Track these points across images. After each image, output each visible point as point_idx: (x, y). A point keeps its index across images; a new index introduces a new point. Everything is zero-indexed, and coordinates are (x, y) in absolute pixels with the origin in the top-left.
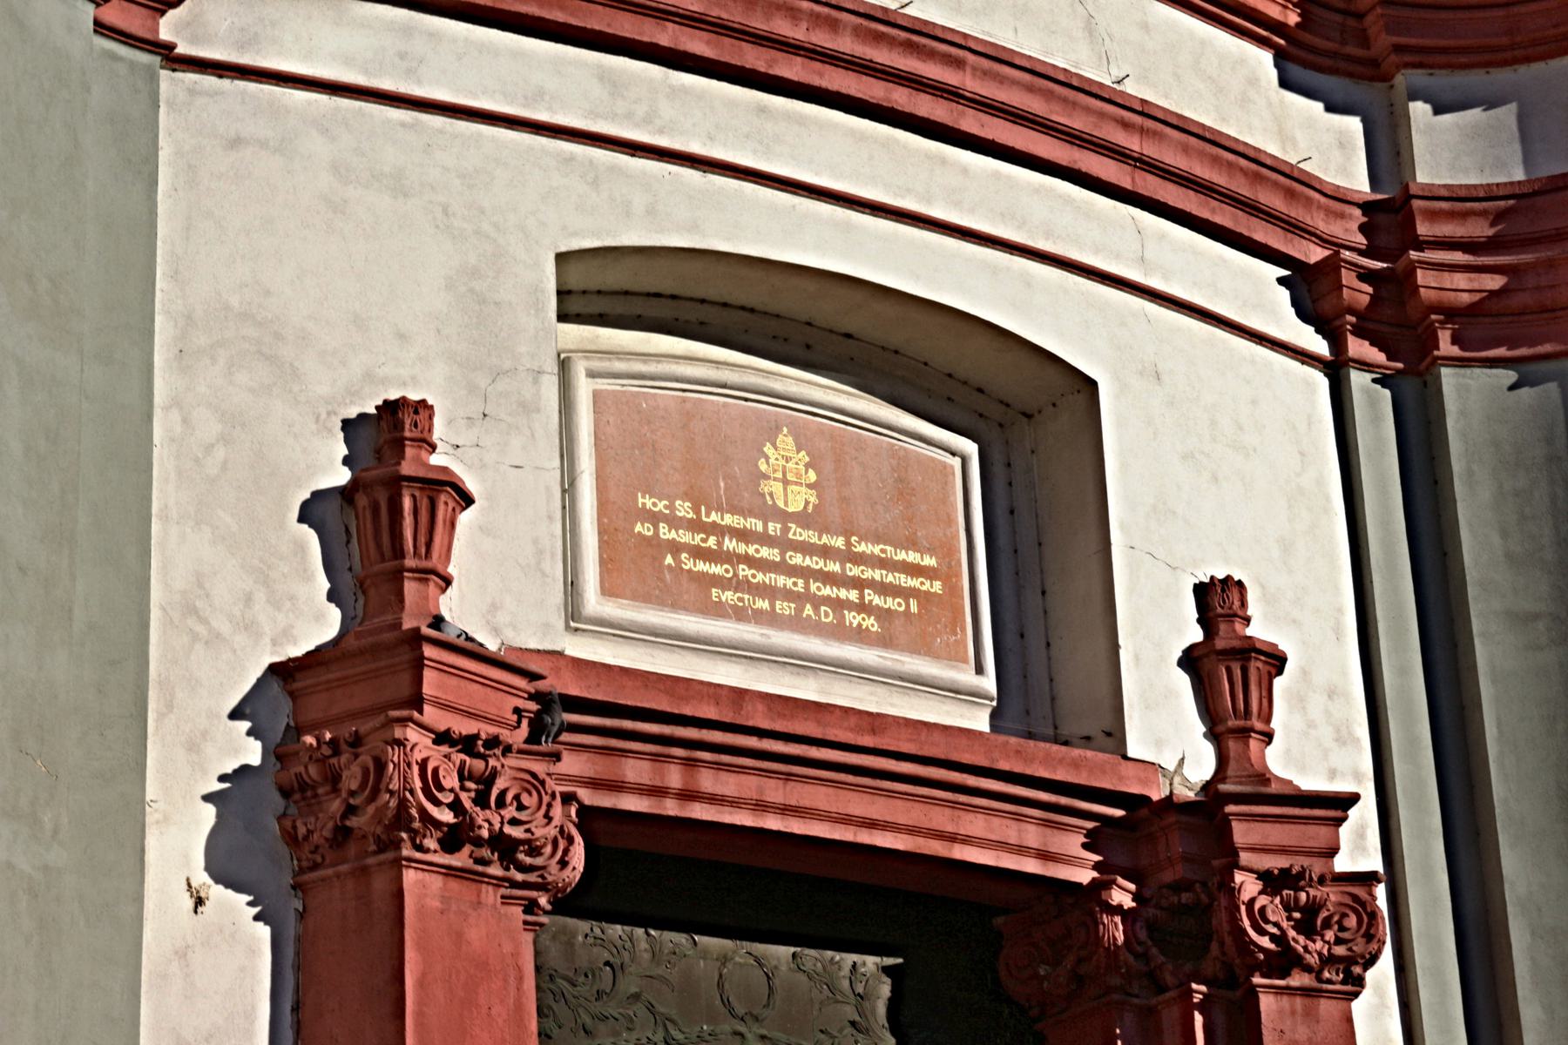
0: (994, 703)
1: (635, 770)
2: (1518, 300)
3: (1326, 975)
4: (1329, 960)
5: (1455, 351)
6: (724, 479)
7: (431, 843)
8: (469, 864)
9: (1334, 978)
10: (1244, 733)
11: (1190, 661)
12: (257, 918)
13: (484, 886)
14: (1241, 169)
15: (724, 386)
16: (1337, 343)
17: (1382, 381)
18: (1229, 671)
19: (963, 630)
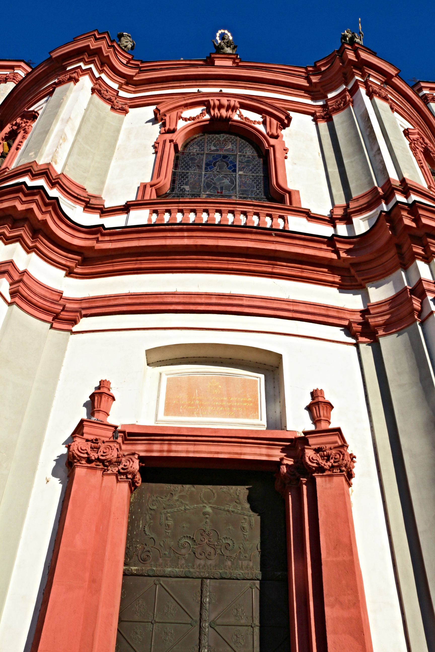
0: (266, 426)
1: (156, 447)
2: (394, 319)
3: (335, 471)
4: (332, 467)
5: (384, 333)
6: (197, 390)
7: (83, 462)
8: (95, 466)
9: (337, 471)
10: (320, 421)
11: (309, 408)
12: (60, 483)
13: (98, 470)
14: (323, 309)
15: (198, 372)
16: (356, 339)
17: (369, 344)
18: (315, 408)
19: (258, 412)
